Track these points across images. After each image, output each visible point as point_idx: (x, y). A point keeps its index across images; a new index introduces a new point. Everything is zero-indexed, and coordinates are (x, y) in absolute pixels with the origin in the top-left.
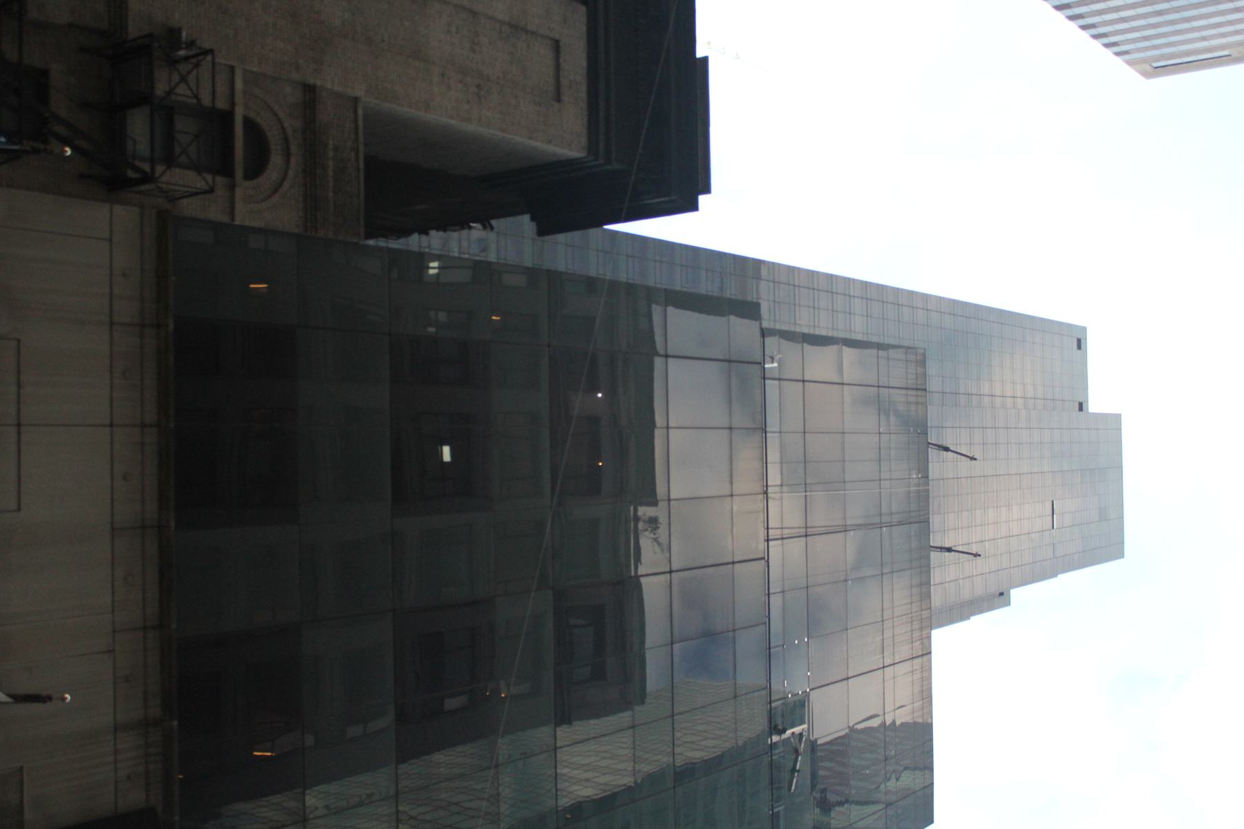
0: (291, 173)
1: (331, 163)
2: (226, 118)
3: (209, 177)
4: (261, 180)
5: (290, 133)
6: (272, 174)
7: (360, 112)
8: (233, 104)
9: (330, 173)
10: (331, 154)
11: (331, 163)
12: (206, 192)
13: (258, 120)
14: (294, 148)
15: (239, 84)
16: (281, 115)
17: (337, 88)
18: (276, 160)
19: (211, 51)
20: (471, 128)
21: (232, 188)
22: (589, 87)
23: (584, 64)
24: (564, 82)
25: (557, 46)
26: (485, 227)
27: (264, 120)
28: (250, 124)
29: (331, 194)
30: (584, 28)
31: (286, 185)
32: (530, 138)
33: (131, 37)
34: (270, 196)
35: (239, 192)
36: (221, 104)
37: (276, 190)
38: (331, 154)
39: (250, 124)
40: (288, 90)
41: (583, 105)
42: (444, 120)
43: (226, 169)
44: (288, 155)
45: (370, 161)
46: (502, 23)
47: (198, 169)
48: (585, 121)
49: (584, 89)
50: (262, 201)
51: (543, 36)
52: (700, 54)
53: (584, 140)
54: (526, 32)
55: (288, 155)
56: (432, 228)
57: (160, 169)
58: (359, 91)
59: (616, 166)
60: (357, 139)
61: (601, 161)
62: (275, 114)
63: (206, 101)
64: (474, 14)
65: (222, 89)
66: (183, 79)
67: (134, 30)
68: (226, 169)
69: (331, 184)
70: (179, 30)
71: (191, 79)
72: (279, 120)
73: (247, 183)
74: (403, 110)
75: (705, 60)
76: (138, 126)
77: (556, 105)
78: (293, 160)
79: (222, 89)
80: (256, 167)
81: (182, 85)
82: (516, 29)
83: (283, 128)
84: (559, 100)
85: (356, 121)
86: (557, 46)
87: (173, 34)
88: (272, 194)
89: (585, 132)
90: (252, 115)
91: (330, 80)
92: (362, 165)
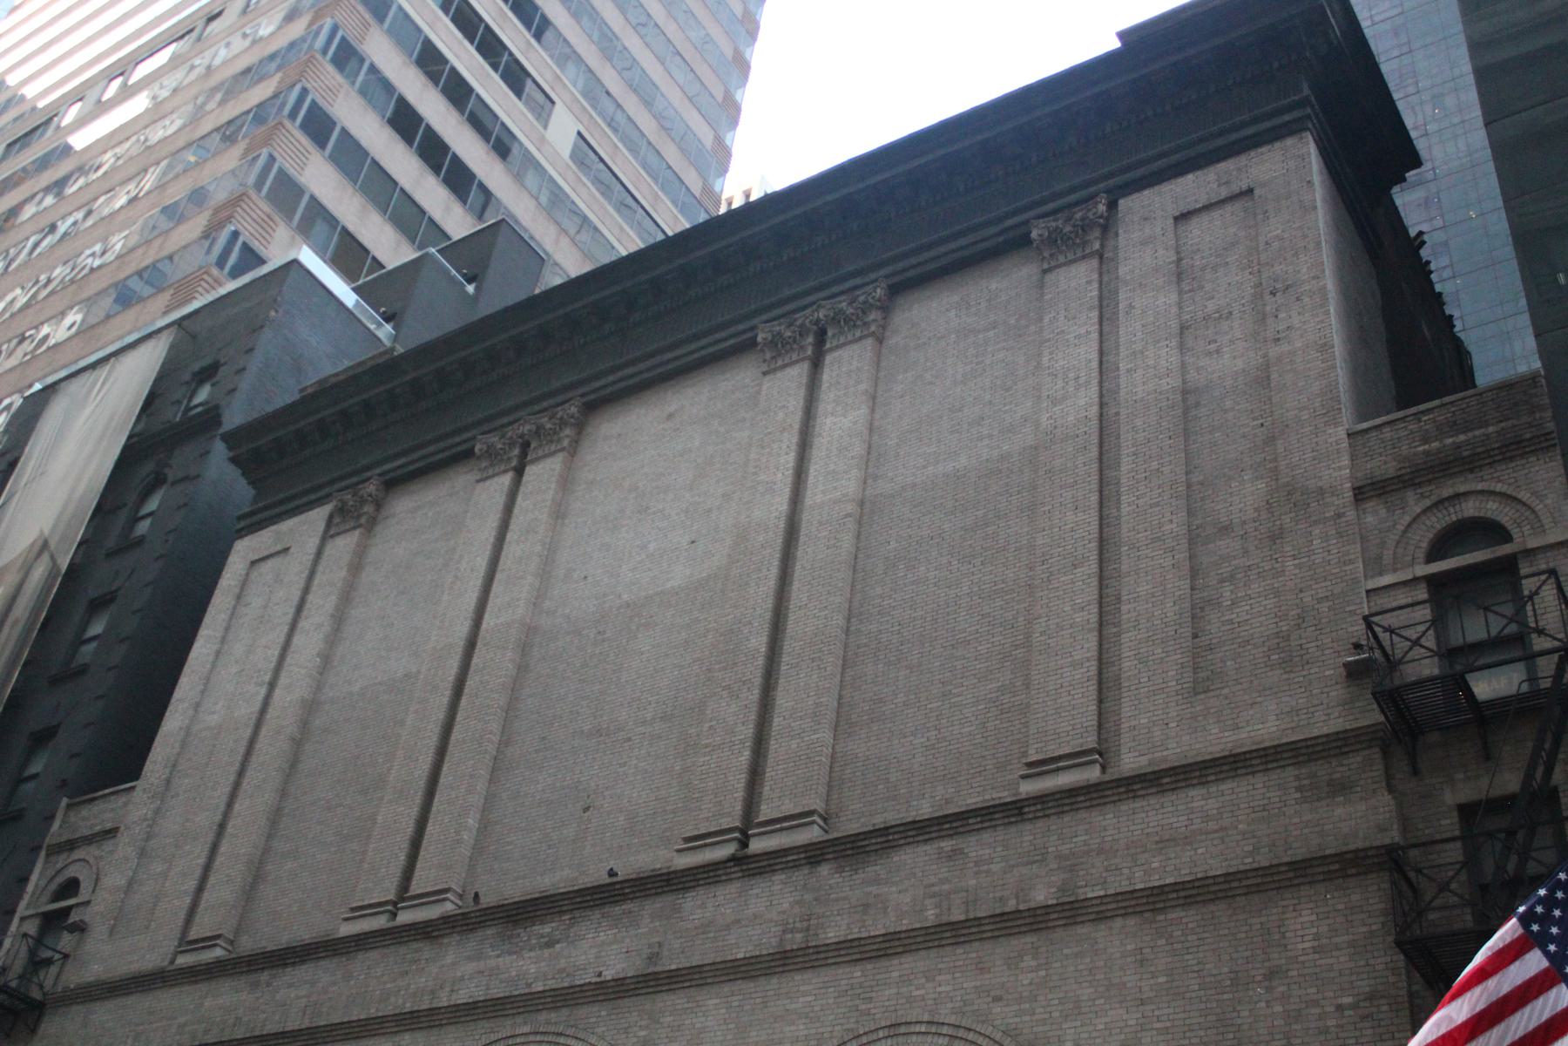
0: (1480, 487)
1: (1449, 441)
2: (1435, 583)
3: (1528, 585)
4: (1504, 520)
5: (1428, 503)
6: (1491, 509)
7: (1365, 425)
8: (1415, 580)
9: (1462, 437)
10: (1435, 445)
11: (1449, 441)
12: (1557, 579)
13: (1424, 545)
14: (1446, 492)
15: (1387, 579)
16: (1408, 519)
17: (1345, 461)
18: (1470, 509)
19: (1366, 618)
20: (1330, 283)
21: (1530, 553)
22: (1219, 161)
23: (1190, 176)
24: (1224, 193)
25: (1183, 217)
26: (1424, 243)
27: (1423, 537)
28: (1433, 555)
29: (1491, 429)
30: (1146, 192)
31: (1499, 487)
32: (1315, 208)
33: (1382, 718)
34: (1524, 504)
35: (1532, 543)
36: (1422, 593)
37: (1515, 499)
38: (1435, 445)
39: (1433, 555)
40: (1369, 519)
41: (1243, 160)
42: (1333, 320)
43: (1507, 569)
44: (1457, 497)
45: (1402, 406)
46: (1181, 293)
47: (1521, 601)
48: (1264, 149)
49: (1222, 166)
50: (1534, 511)
51: (1177, 239)
52: (1116, 44)
53: (1289, 142)
54: (1179, 260)
55: (1457, 497)
56: (1443, 312)
57: (1540, 643)
58: (1341, 433)
59: (1306, 91)
60: (1403, 419)
61: (1309, 110)
62: (1409, 525)
63: (1425, 613)
64: (1183, 328)
65: (1402, 598)
66: (1416, 643)
67: (1373, 716)
68: (1507, 569)
69: (1477, 433)
70: (1346, 665)
71: (1412, 633)
72: (1414, 520)
73: (1515, 533)
74: (1342, 376)
75: (1122, 35)
76: (1486, 687)
77: (1257, 192)
78: (1462, 489)
79: (1402, 598)
80: (1492, 531)
81: (1423, 641)
82: (1180, 273)
83: (1425, 511)
84: (1250, 191)
85: (1376, 427)
86: (1183, 217)
87: (1354, 673)
88: (1520, 501)
89: (1277, 145)
90: (1421, 555)
91: (1339, 472)
92: (1436, 402)
